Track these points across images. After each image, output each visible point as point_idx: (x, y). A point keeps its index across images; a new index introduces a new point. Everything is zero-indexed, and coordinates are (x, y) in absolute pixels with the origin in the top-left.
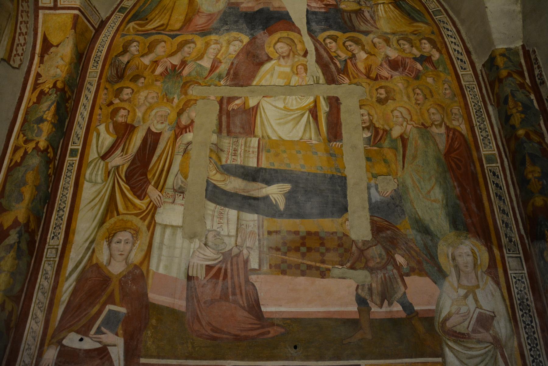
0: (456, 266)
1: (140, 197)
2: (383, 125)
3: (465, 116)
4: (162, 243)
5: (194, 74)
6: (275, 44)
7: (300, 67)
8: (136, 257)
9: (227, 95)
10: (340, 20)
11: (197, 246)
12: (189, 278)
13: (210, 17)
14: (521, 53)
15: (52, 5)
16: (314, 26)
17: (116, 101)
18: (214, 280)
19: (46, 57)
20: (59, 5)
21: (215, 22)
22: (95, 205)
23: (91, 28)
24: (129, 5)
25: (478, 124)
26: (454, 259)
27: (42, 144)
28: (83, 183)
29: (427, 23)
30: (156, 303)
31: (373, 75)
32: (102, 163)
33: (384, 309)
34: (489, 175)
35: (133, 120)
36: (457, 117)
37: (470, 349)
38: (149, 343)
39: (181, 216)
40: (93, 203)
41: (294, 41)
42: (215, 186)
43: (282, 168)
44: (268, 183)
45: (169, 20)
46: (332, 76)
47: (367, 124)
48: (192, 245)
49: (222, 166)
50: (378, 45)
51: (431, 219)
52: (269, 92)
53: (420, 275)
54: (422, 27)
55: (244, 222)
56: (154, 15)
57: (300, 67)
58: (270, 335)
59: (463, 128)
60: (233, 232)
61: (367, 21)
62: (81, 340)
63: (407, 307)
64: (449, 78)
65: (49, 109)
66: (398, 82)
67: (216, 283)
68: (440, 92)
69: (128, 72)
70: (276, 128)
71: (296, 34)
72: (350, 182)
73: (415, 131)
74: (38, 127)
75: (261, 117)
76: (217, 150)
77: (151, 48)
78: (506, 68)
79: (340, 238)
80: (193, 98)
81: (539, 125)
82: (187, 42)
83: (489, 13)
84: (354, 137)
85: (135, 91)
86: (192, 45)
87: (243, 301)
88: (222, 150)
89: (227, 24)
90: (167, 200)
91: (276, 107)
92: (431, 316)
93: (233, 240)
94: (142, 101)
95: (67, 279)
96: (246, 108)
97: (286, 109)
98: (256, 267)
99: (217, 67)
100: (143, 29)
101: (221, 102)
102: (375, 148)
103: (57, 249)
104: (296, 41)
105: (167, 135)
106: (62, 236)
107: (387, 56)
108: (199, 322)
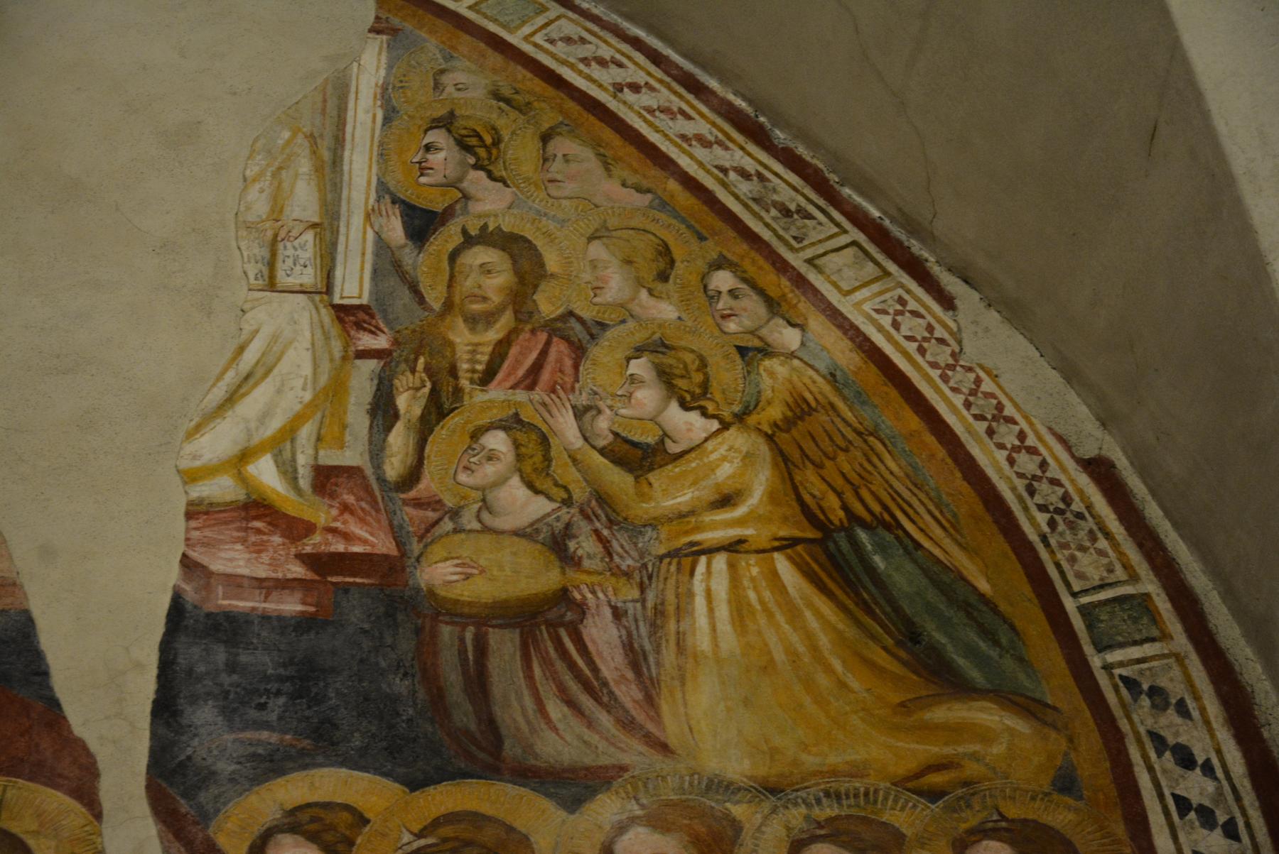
10: (400, 686)
16: (213, 737)
29: (1031, 707)
61: (595, 687)
71: (56, 801)
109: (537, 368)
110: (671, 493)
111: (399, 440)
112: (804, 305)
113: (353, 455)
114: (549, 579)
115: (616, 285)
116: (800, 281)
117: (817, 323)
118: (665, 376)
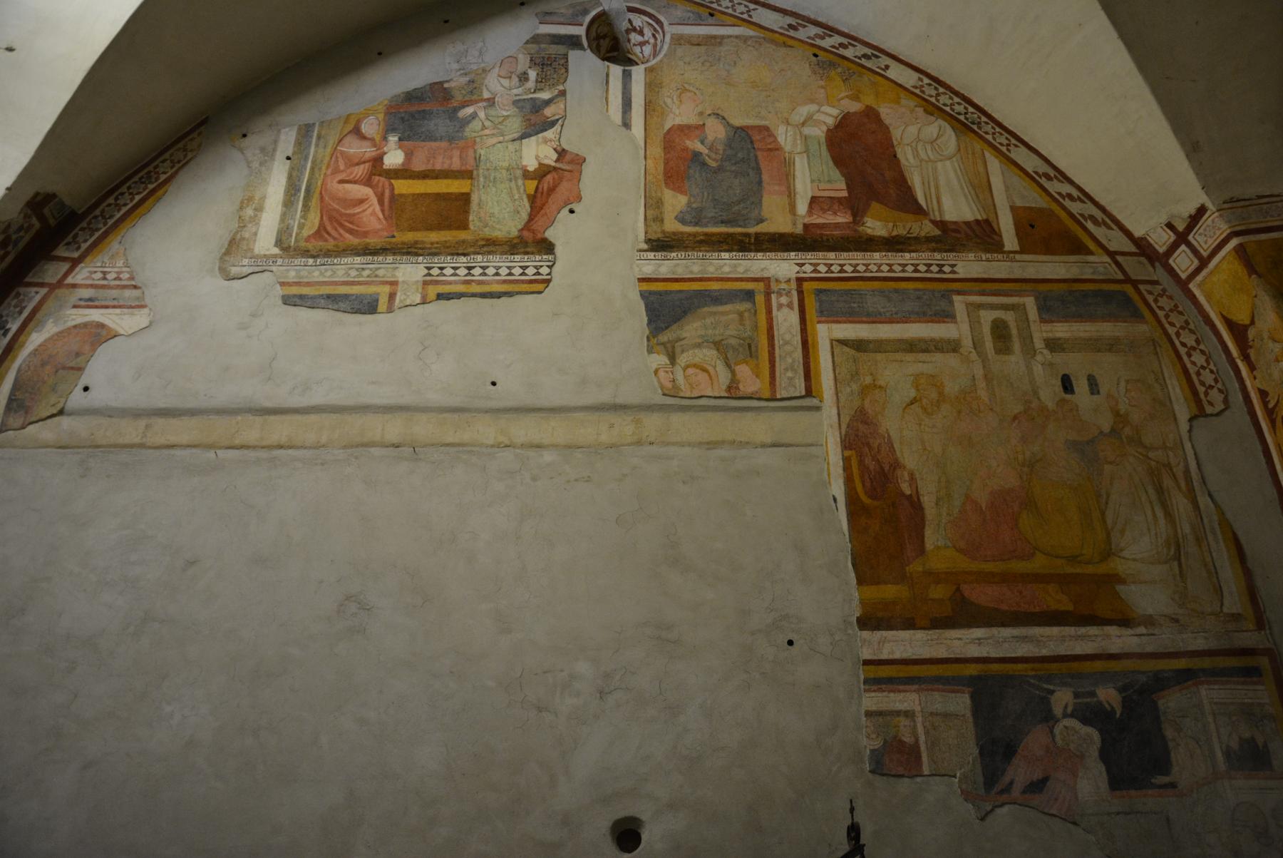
19: (1252, 353)
20: (1205, 254)
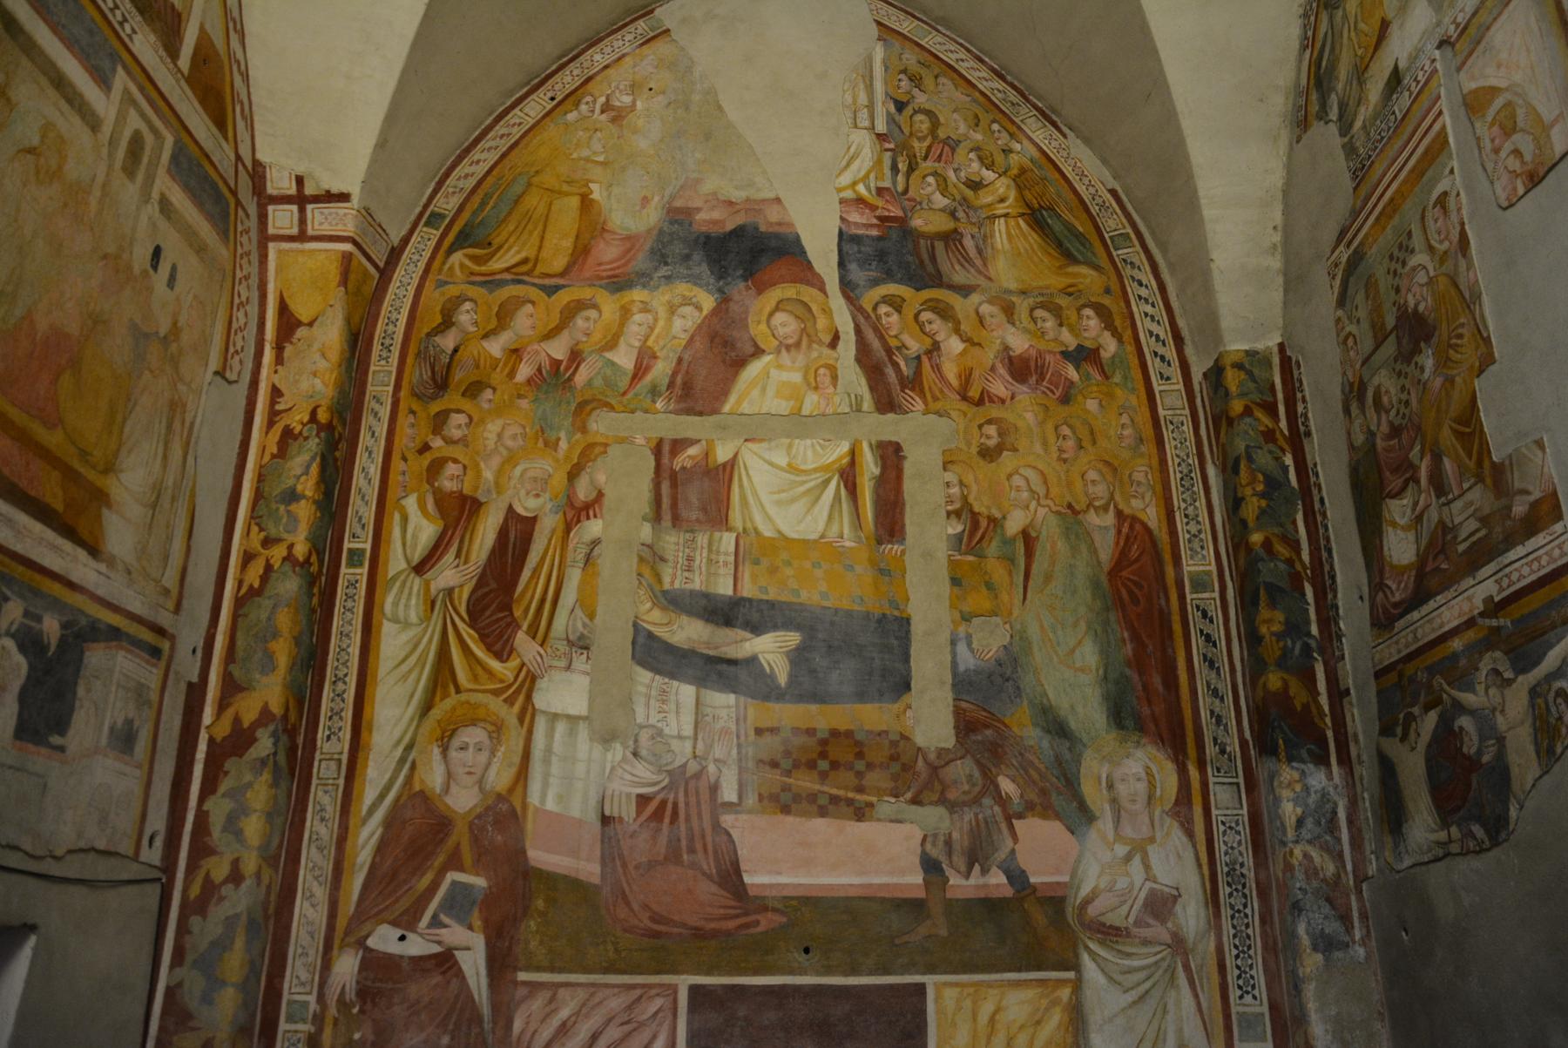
0: (1114, 801)
1: (499, 656)
2: (988, 508)
3: (1159, 488)
4: (549, 750)
5: (598, 382)
6: (771, 315)
7: (822, 371)
8: (499, 777)
9: (670, 435)
10: (910, 259)
11: (619, 757)
12: (606, 820)
13: (628, 245)
14: (1276, 360)
15: (295, 231)
16: (857, 274)
17: (437, 443)
18: (653, 825)
19: (289, 350)
20: (310, 232)
21: (640, 256)
22: (410, 671)
23: (372, 270)
24: (449, 207)
25: (1183, 505)
26: (1110, 786)
27: (300, 551)
28: (381, 624)
29: (1097, 268)
30: (544, 867)
31: (974, 393)
32: (417, 581)
33: (972, 881)
34: (1194, 616)
35: (476, 488)
36: (1140, 490)
37: (1129, 955)
38: (533, 944)
39: (586, 696)
40: (405, 667)
41: (810, 310)
42: (650, 635)
43: (783, 599)
44: (756, 629)
45: (540, 248)
46: (889, 394)
47: (957, 505)
48: (609, 756)
49: (665, 593)
50: (988, 320)
51: (1072, 707)
52: (758, 430)
53: (1044, 817)
54: (1086, 276)
55: (709, 710)
56: (505, 234)
57: (822, 371)
58: (759, 929)
59: (1152, 516)
60: (688, 730)
61: (969, 260)
62: (402, 938)
63: (1017, 877)
64: (1134, 400)
65: (306, 473)
66: (1025, 408)
67: (659, 830)
68: (1112, 432)
69: (458, 375)
70: (772, 510)
71: (815, 292)
72: (917, 629)
73: (1053, 520)
74: (288, 512)
75: (741, 486)
76: (652, 558)
77: (503, 317)
78: (1242, 395)
79: (894, 744)
80: (602, 440)
81: (1294, 522)
82: (579, 306)
83: (1216, 274)
84: (929, 532)
85: (475, 419)
86: (593, 314)
87: (709, 865)
88: (663, 559)
89: (666, 264)
90: (556, 663)
91: (771, 464)
92: (1059, 893)
93: (688, 745)
94: (491, 444)
95: (364, 821)
96: (711, 465)
97: (792, 469)
98: (734, 798)
99: (648, 369)
100: (483, 269)
101: (657, 451)
102: (971, 558)
103: (339, 761)
104: (814, 308)
105: (549, 523)
106: (347, 735)
107: (1007, 348)
108: (628, 904)
109: (940, 156)
110: (986, 198)
111: (900, 178)
112: (1021, 136)
113: (887, 184)
114: (951, 225)
115: (963, 128)
116: (1019, 128)
117: (1025, 142)
118: (980, 159)
